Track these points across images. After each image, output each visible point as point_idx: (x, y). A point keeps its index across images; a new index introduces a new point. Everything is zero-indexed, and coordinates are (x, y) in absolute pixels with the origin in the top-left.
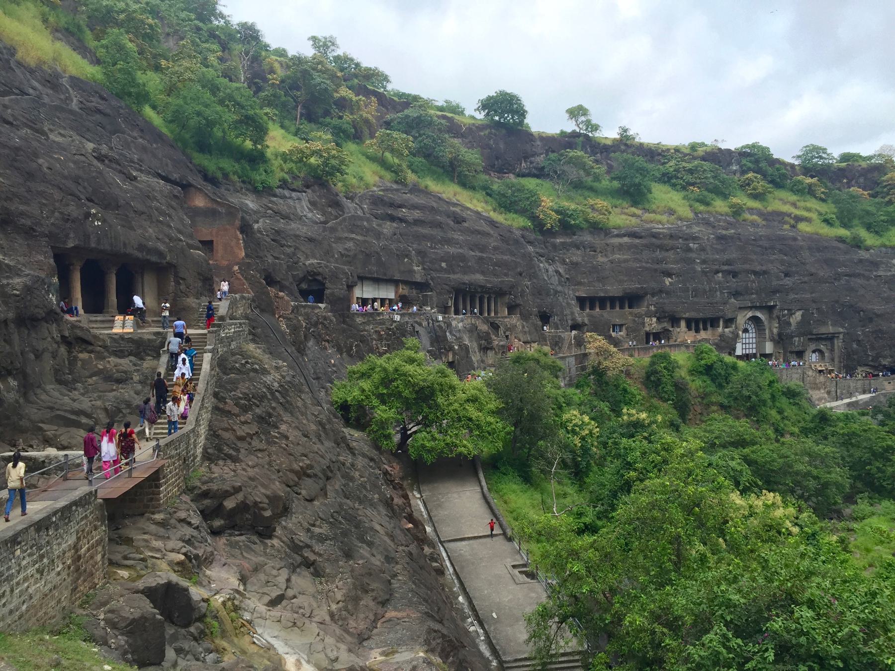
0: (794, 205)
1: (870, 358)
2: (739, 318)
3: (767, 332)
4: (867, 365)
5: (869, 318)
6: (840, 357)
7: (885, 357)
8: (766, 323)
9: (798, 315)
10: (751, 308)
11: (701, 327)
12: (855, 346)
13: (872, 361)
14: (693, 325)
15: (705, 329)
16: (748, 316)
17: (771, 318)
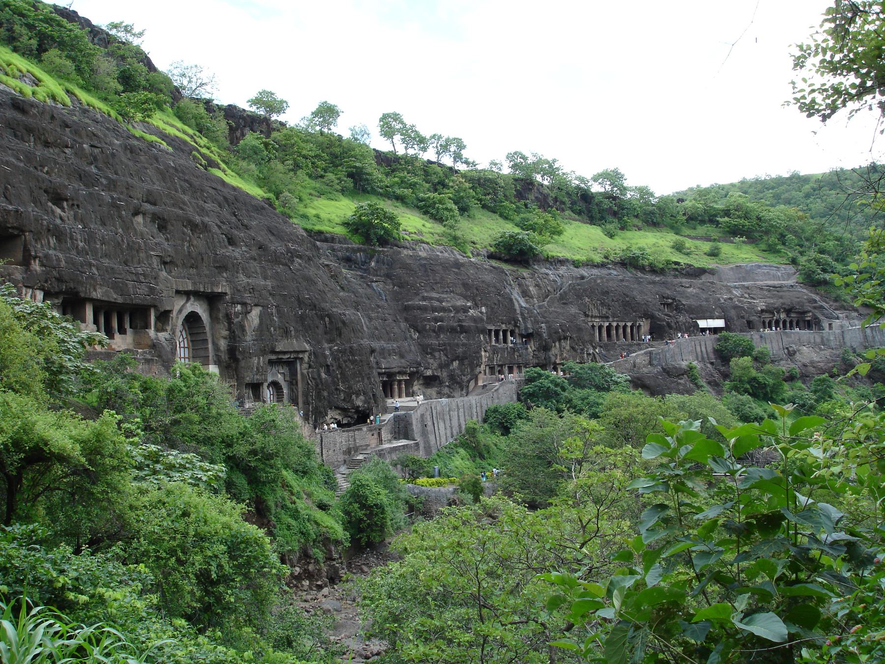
0: (192, 137)
1: (342, 396)
2: (175, 313)
3: (210, 346)
4: (337, 408)
5: (336, 328)
6: (306, 395)
7: (358, 395)
8: (207, 328)
9: (255, 312)
10: (188, 294)
11: (115, 324)
12: (323, 375)
13: (344, 400)
14: (102, 321)
15: (122, 331)
16: (185, 313)
17: (213, 318)
